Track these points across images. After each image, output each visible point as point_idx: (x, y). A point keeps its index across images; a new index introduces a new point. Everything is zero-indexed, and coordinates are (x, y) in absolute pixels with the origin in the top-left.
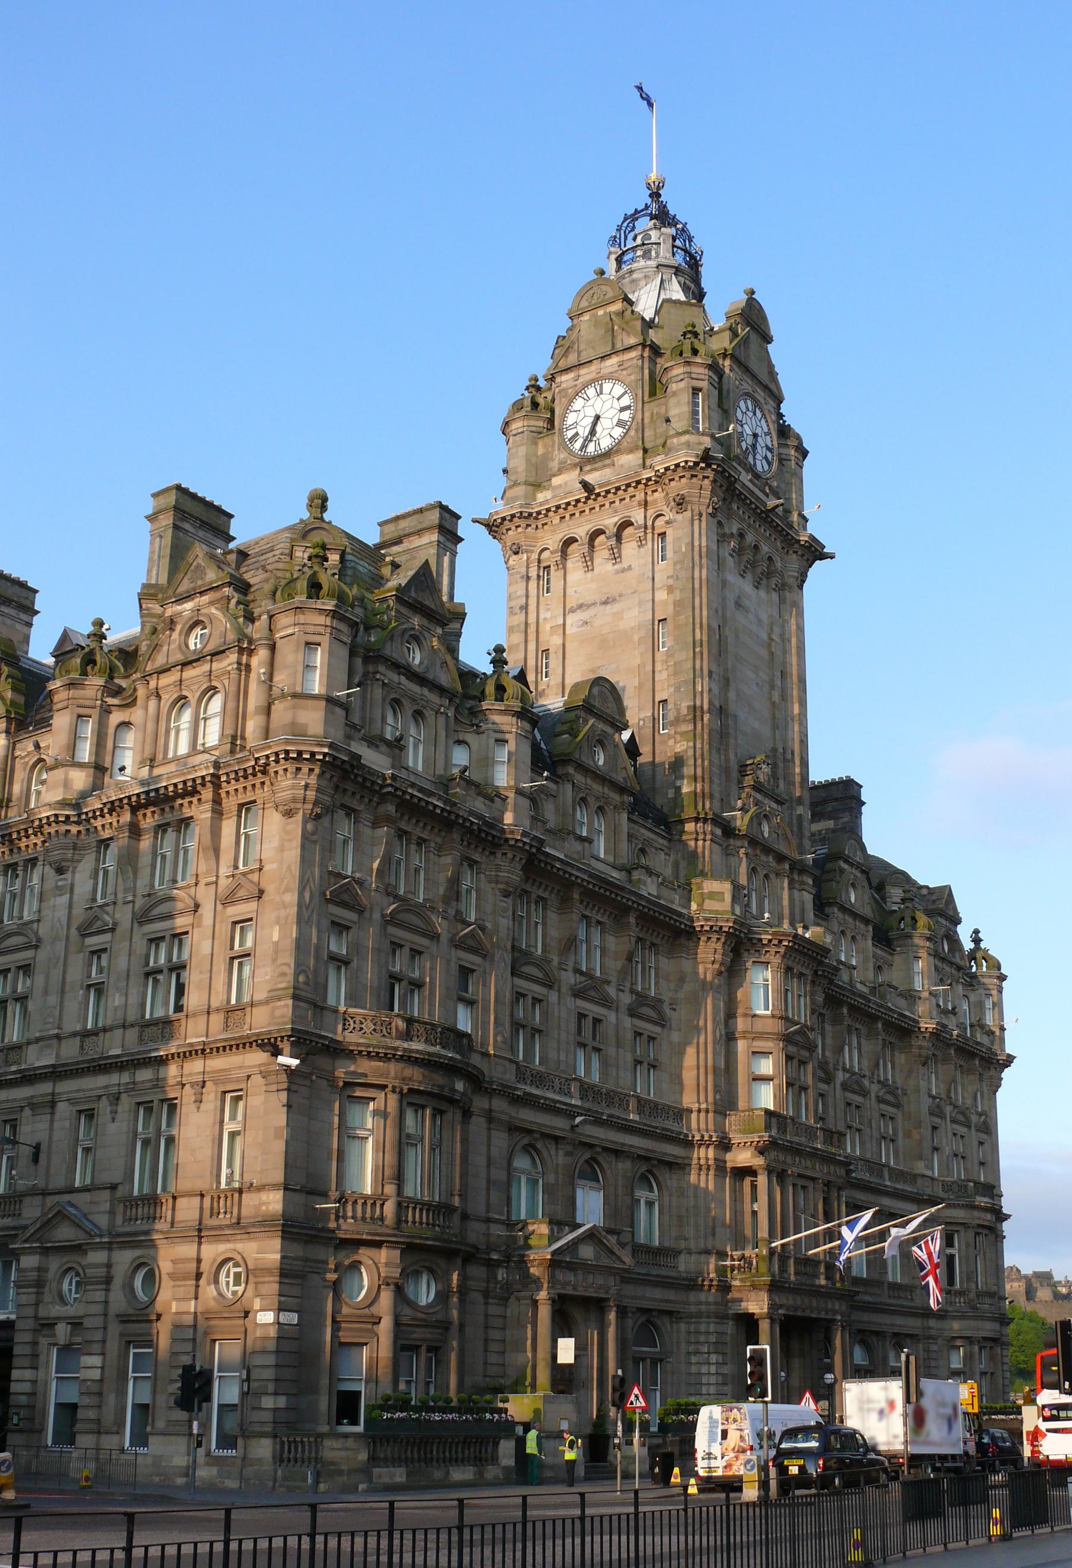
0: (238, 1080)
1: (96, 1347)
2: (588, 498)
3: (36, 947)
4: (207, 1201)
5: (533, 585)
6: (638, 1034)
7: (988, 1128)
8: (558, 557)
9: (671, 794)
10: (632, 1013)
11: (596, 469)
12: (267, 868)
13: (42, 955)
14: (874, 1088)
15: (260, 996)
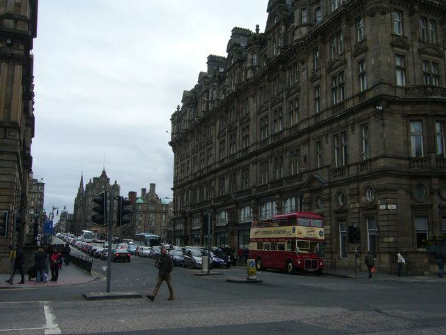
0: (365, 119)
1: (328, 223)
3: (299, 91)
4: (359, 166)
12: (368, 38)
13: (301, 93)
15: (370, 87)
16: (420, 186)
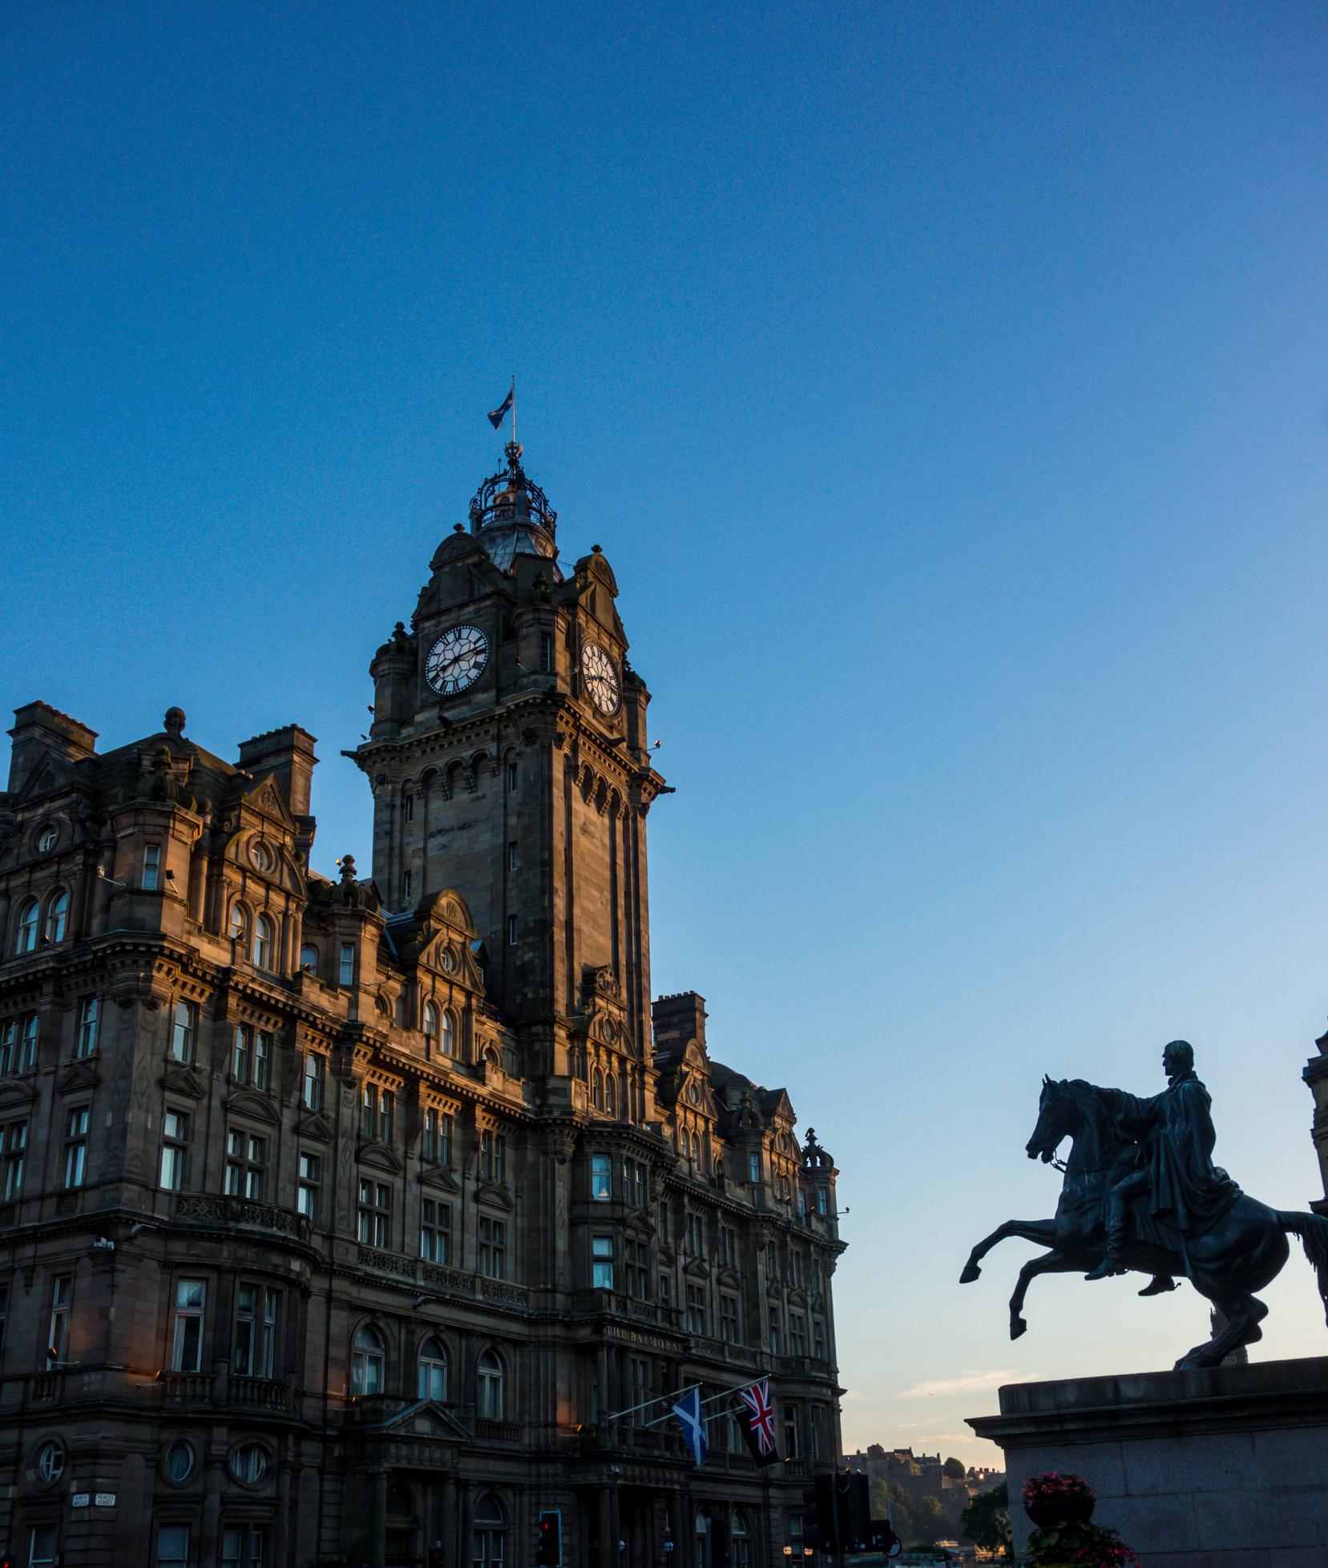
2: (446, 733)
5: (397, 813)
6: (484, 1221)
7: (824, 1307)
8: (419, 786)
9: (519, 1000)
10: (477, 1198)
11: (454, 707)
14: (715, 1271)
16: (179, 1445)
